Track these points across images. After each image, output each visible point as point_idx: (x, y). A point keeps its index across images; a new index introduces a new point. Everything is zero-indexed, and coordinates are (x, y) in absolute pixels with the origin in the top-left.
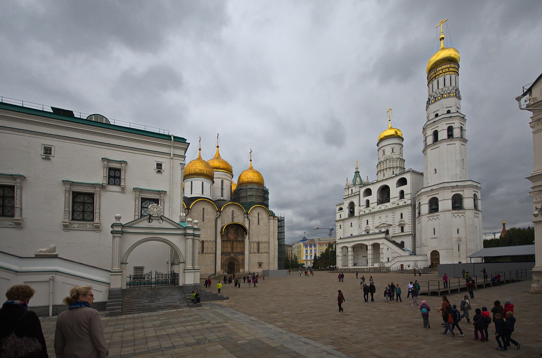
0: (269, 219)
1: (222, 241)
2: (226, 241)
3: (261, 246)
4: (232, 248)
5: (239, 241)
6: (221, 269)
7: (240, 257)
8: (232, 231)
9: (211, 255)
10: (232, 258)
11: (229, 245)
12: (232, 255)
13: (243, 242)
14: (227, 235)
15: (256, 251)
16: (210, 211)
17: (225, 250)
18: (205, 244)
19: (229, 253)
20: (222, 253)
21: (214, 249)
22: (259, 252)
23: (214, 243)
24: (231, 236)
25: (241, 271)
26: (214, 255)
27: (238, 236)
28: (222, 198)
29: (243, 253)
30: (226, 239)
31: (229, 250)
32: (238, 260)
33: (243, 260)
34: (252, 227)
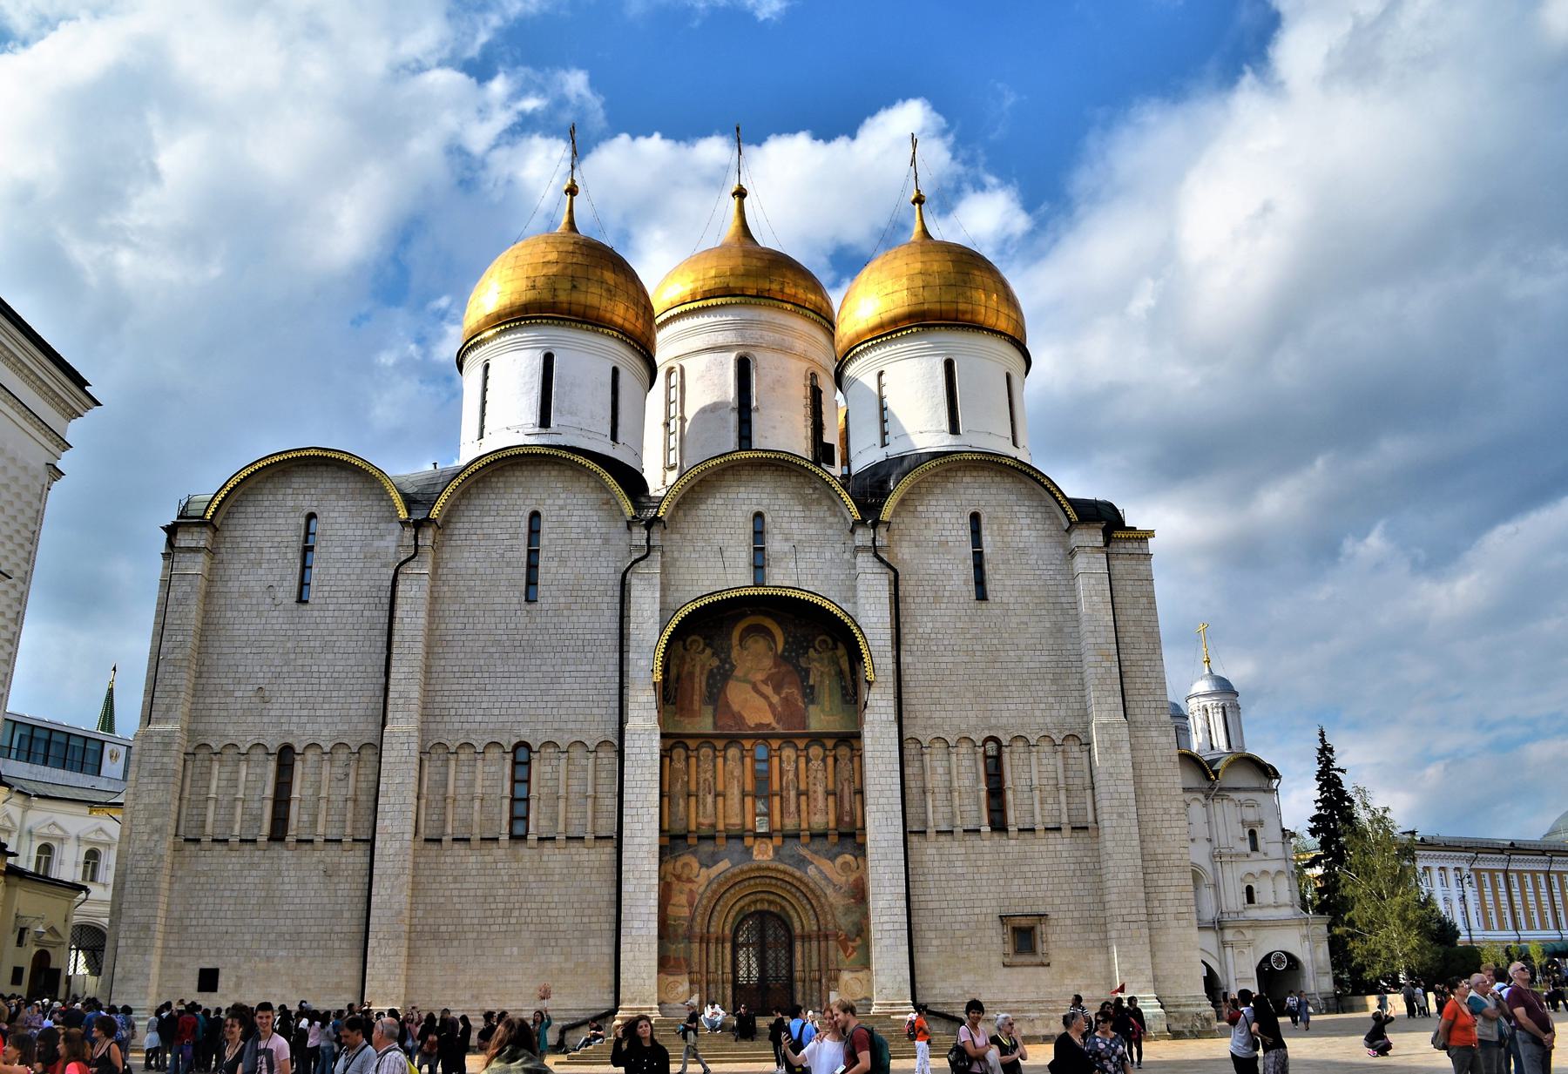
0: (1072, 554)
1: (672, 743)
2: (706, 739)
3: (1018, 774)
5: (817, 738)
7: (824, 872)
9: (580, 853)
10: (762, 874)
12: (763, 854)
13: (850, 740)
14: (715, 696)
17: (701, 815)
18: (541, 770)
21: (610, 803)
23: (608, 758)
24: (753, 703)
26: (609, 849)
27: (810, 694)
31: (733, 812)
32: (809, 895)
33: (860, 894)
34: (920, 624)
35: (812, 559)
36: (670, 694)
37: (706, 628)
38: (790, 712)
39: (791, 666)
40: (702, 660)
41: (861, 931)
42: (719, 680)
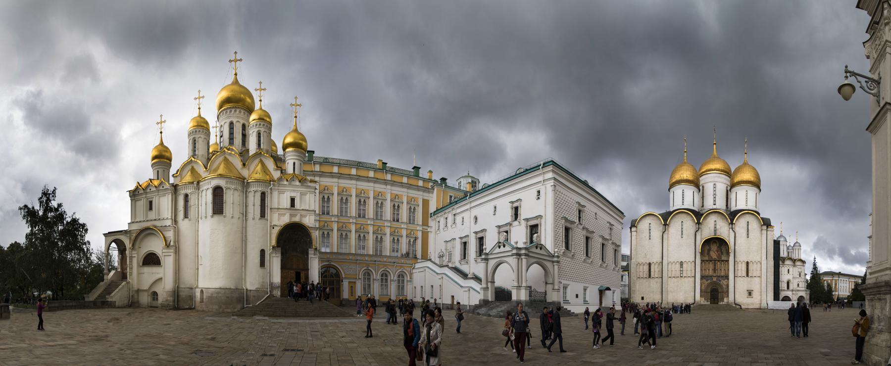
1: (702, 261)
4: (715, 270)
6: (701, 296)
7: (724, 282)
8: (714, 247)
11: (711, 266)
12: (715, 279)
13: (728, 261)
14: (708, 253)
15: (744, 274)
16: (689, 223)
17: (707, 273)
19: (711, 276)
20: (702, 277)
22: (747, 275)
24: (714, 255)
25: (725, 300)
27: (722, 253)
28: (714, 207)
29: (727, 277)
30: (707, 258)
31: (711, 272)
32: (721, 286)
35: (724, 231)
36: (702, 253)
37: (708, 242)
38: (719, 257)
39: (720, 247)
40: (707, 247)
41: (728, 291)
42: (709, 250)
